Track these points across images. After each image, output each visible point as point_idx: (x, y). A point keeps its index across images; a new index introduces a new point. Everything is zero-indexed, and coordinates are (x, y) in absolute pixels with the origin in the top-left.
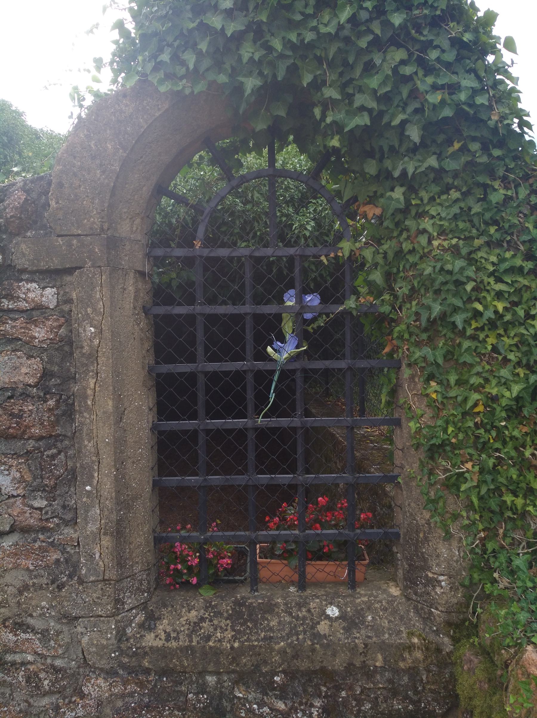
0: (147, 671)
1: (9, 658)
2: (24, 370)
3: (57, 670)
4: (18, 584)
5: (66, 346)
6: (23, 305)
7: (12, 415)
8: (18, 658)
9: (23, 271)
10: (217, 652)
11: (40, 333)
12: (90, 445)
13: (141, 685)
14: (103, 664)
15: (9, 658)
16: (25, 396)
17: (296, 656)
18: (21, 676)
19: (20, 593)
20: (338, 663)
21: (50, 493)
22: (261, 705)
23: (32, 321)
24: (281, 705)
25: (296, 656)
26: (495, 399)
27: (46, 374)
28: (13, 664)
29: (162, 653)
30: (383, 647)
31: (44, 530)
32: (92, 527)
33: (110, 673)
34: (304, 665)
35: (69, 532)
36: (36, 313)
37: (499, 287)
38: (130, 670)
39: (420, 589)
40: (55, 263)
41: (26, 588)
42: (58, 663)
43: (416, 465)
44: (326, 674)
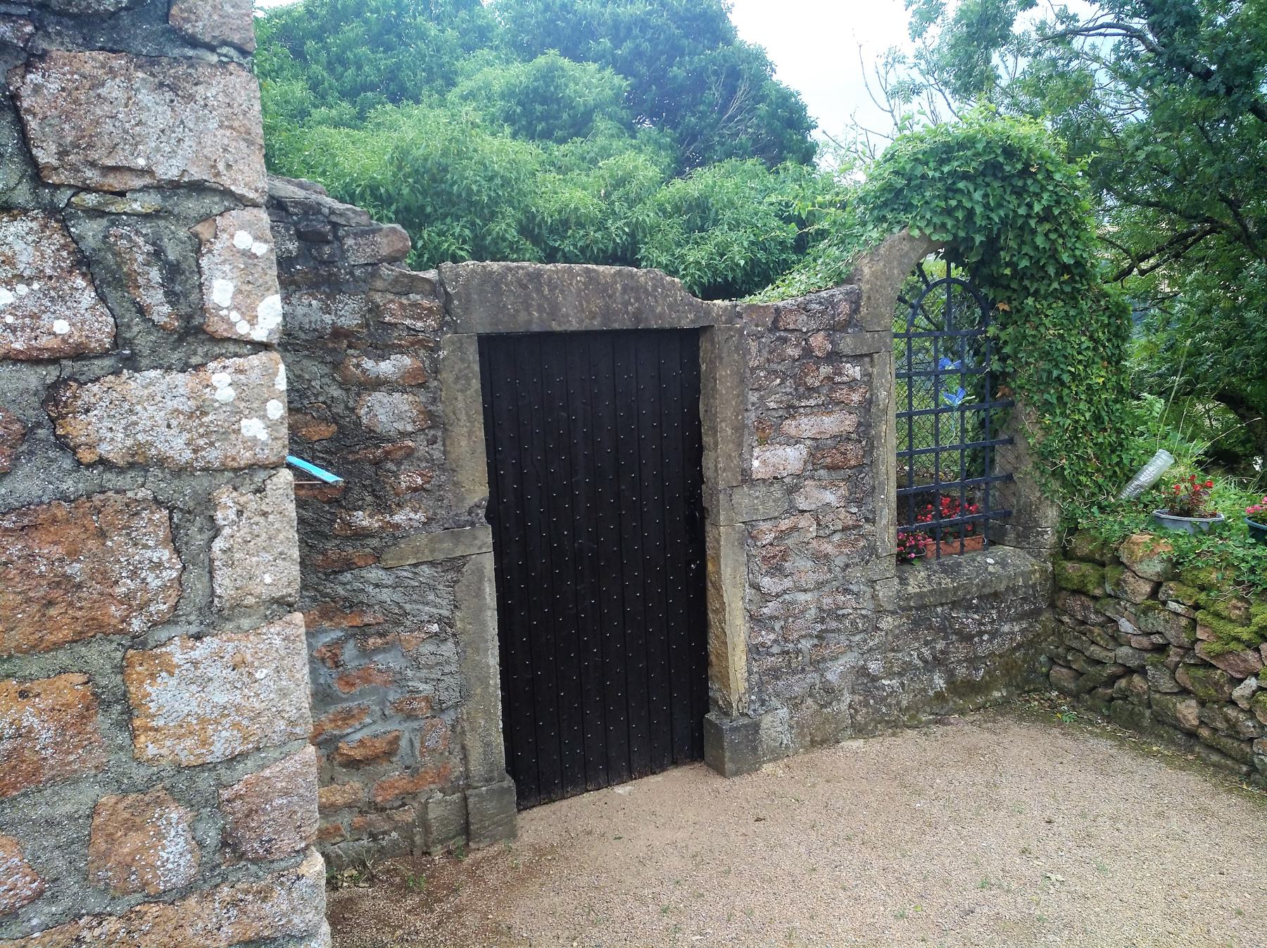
0: (911, 608)
1: (840, 612)
2: (847, 422)
3: (864, 616)
4: (842, 565)
5: (868, 405)
6: (845, 379)
7: (842, 453)
8: (845, 611)
9: (846, 356)
10: (947, 590)
11: (856, 397)
12: (883, 469)
13: (908, 618)
14: (890, 608)
15: (840, 612)
16: (849, 439)
17: (984, 586)
18: (847, 622)
19: (844, 570)
20: (1002, 587)
21: (859, 503)
22: (967, 618)
23: (852, 389)
24: (976, 617)
25: (984, 586)
26: (1077, 422)
27: (860, 424)
28: (843, 615)
29: (921, 596)
30: (1023, 574)
31: (855, 527)
32: (884, 522)
33: (893, 613)
34: (987, 591)
35: (868, 527)
36: (852, 385)
37: (1080, 357)
38: (903, 609)
39: (1032, 539)
40: (865, 350)
41: (847, 566)
42: (863, 612)
43: (1030, 466)
44: (996, 595)
